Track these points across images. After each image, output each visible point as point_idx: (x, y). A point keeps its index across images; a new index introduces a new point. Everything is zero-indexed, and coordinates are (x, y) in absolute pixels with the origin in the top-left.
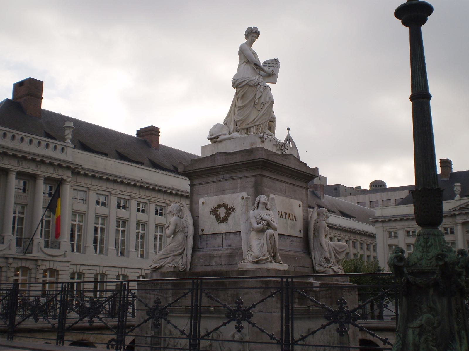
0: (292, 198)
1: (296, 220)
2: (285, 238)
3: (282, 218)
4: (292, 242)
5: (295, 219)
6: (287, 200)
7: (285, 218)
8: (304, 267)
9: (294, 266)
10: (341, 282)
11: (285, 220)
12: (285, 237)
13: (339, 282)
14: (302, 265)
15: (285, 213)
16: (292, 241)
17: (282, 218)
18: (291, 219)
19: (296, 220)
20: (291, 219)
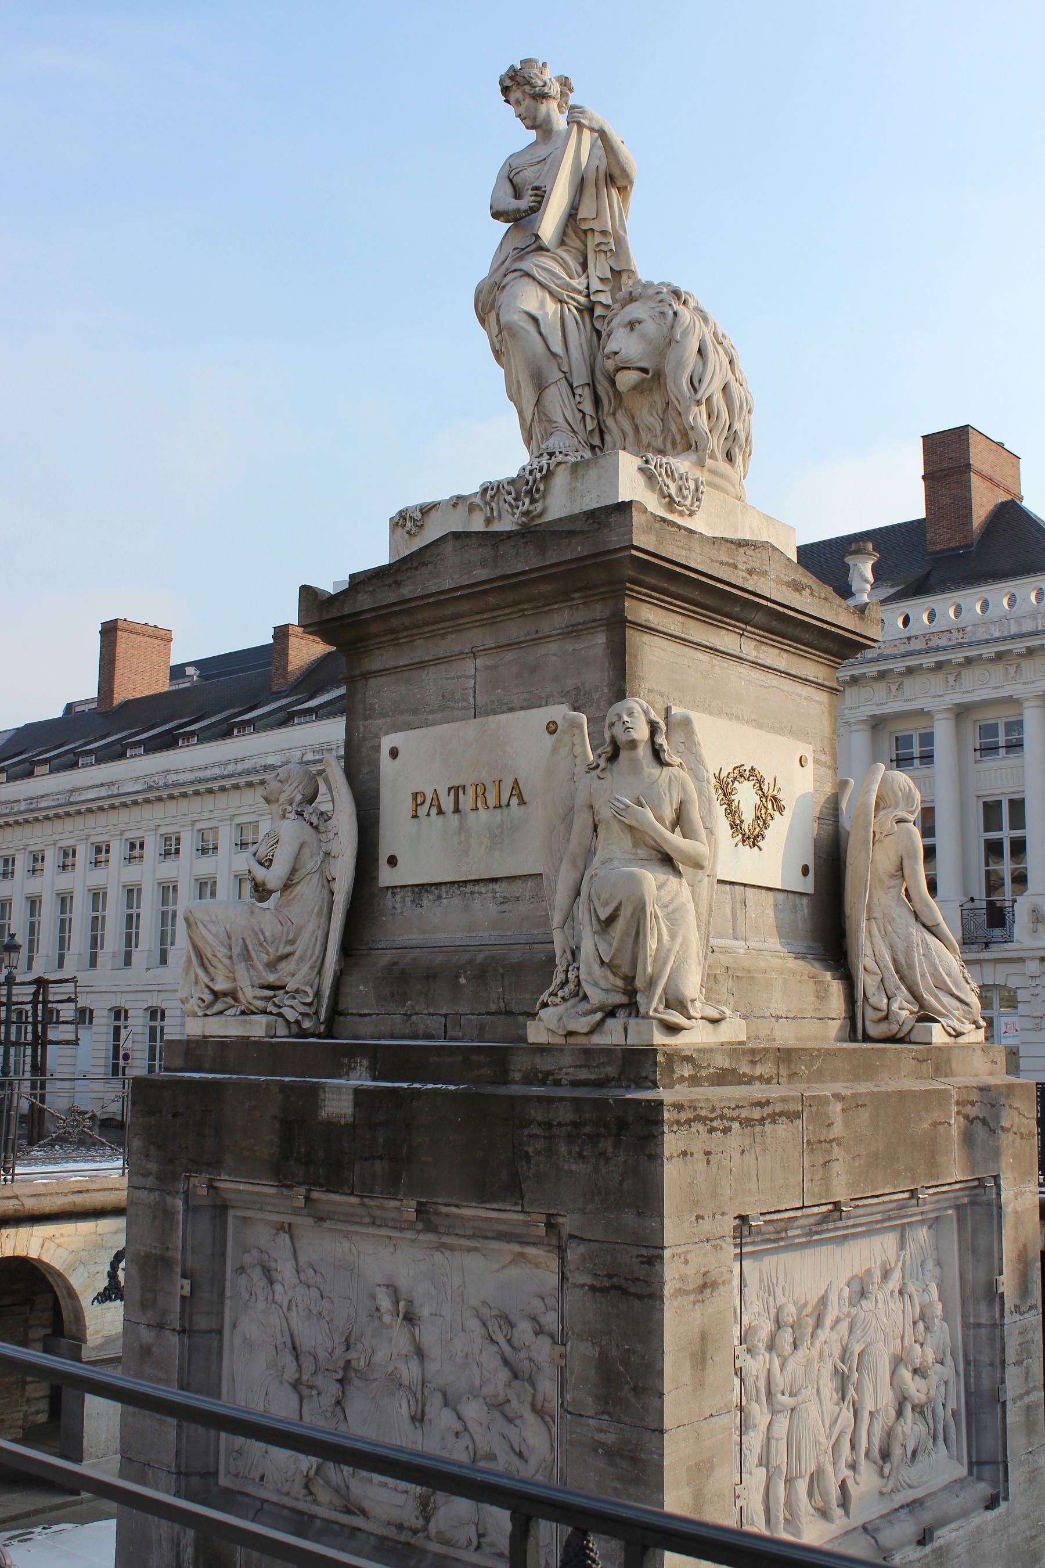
0: (511, 710)
1: (522, 802)
2: (464, 895)
3: (440, 812)
4: (503, 908)
5: (515, 801)
6: (469, 730)
7: (457, 810)
8: (509, 1013)
9: (445, 1016)
10: (575, 1084)
11: (454, 820)
12: (470, 888)
13: (557, 1083)
14: (493, 1008)
15: (457, 789)
16: (505, 901)
17: (440, 812)
18: (492, 801)
19: (522, 802)
20: (492, 801)
